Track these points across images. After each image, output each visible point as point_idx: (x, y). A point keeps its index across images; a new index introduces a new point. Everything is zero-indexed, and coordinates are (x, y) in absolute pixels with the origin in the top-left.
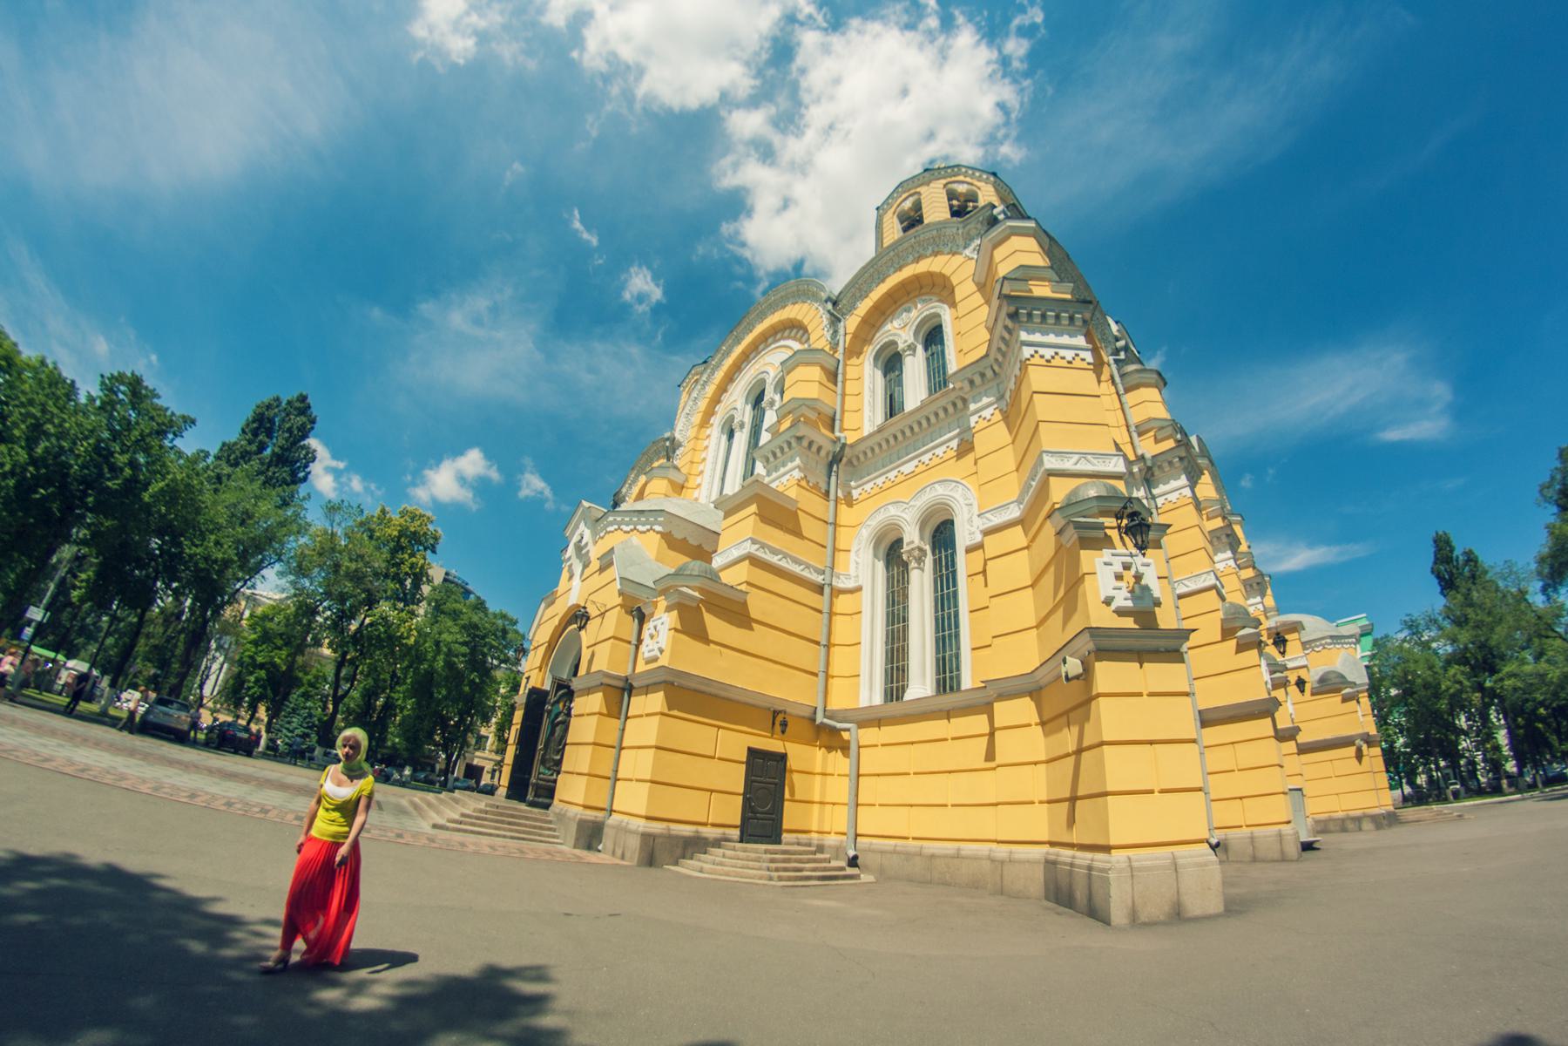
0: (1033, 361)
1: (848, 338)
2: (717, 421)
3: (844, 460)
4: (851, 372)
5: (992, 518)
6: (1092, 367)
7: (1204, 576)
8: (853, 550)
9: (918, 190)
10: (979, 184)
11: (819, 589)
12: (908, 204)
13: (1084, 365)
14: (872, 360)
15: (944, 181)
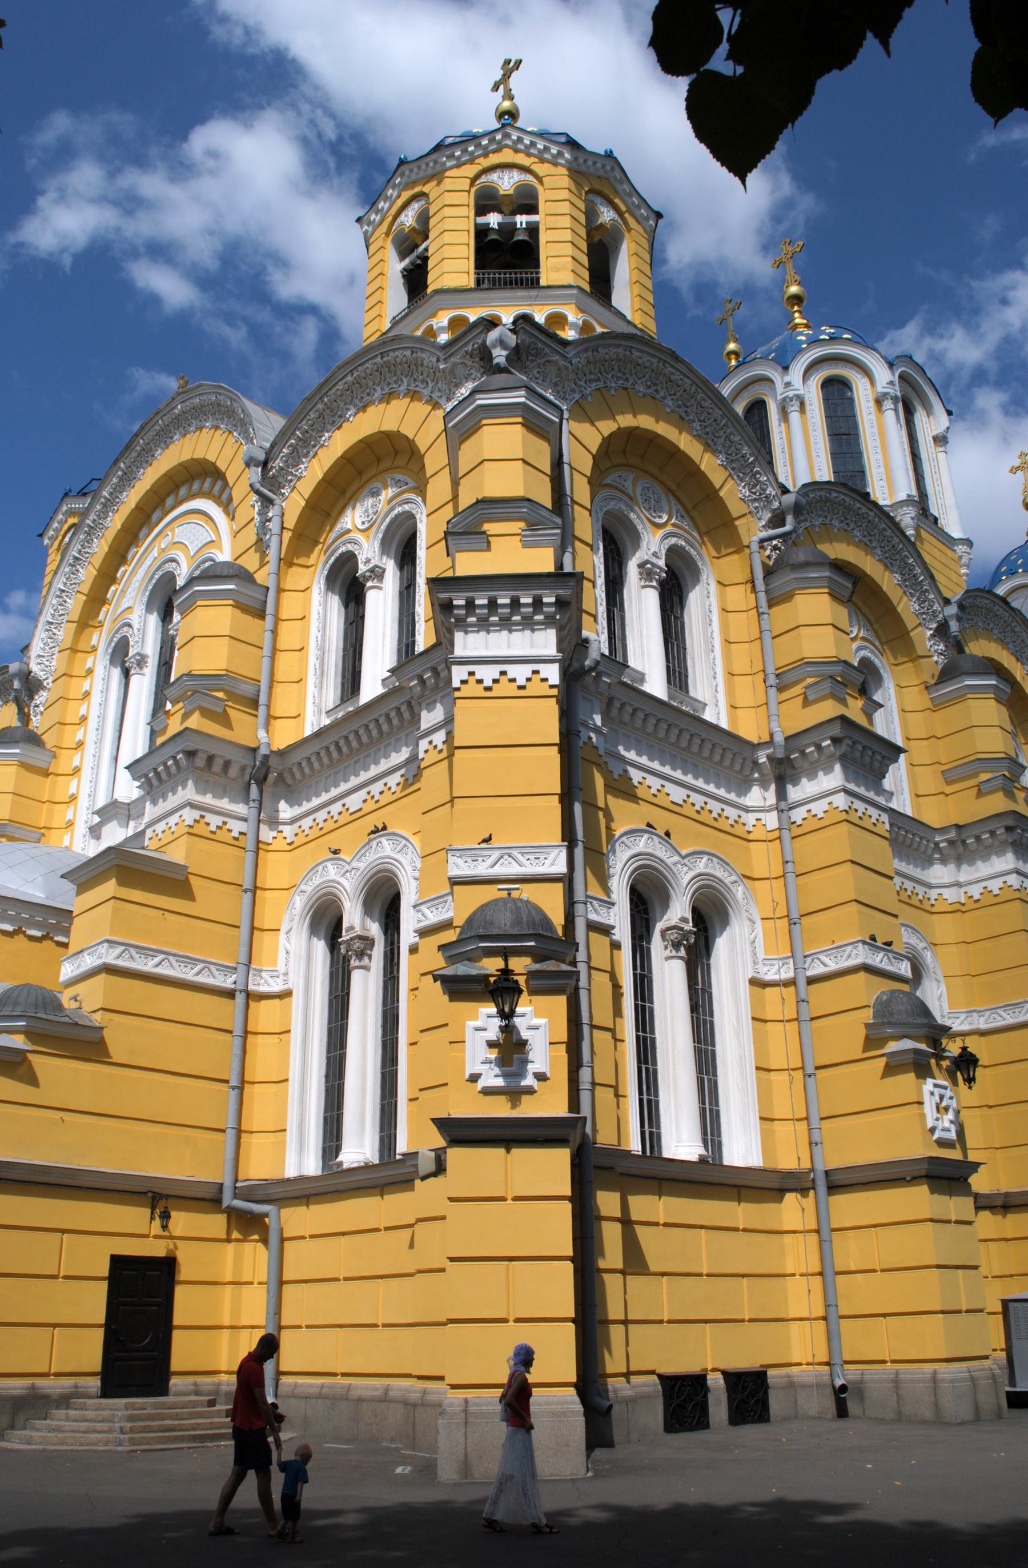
0: (466, 691)
1: (287, 535)
2: (101, 639)
3: (273, 776)
4: (290, 605)
5: (427, 912)
6: (555, 692)
7: (849, 948)
8: (283, 930)
9: (426, 189)
10: (541, 169)
11: (230, 994)
12: (409, 219)
13: (544, 689)
14: (323, 581)
15: (470, 170)
